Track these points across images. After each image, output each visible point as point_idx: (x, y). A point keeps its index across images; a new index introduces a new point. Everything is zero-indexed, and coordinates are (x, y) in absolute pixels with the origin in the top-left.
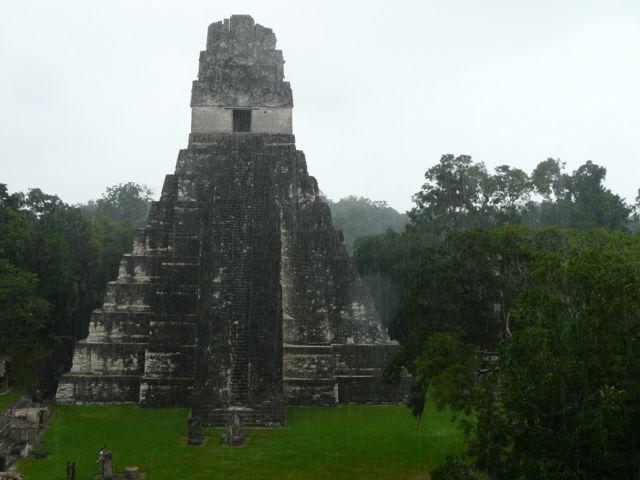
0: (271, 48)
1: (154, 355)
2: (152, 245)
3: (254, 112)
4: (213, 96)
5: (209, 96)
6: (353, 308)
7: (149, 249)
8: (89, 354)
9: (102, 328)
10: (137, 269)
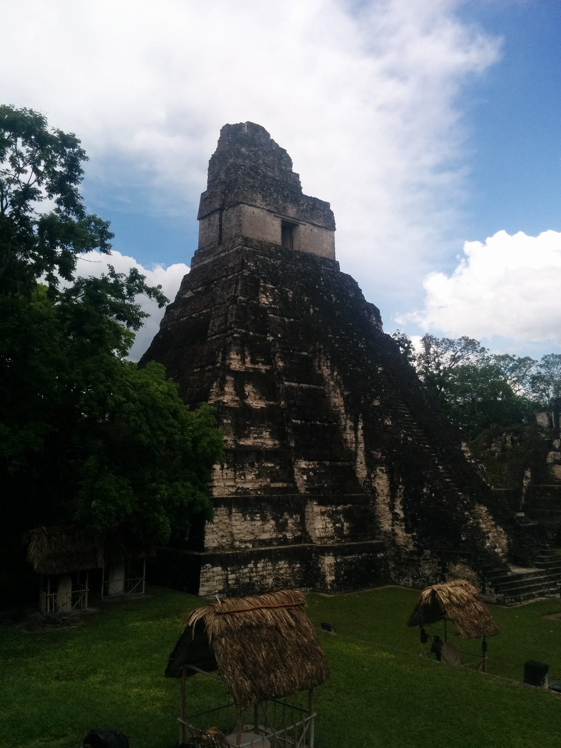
0: (288, 169)
1: (323, 509)
2: (253, 362)
3: (302, 228)
4: (264, 197)
5: (260, 197)
6: (463, 449)
7: (249, 365)
8: (230, 514)
9: (230, 473)
10: (248, 388)
